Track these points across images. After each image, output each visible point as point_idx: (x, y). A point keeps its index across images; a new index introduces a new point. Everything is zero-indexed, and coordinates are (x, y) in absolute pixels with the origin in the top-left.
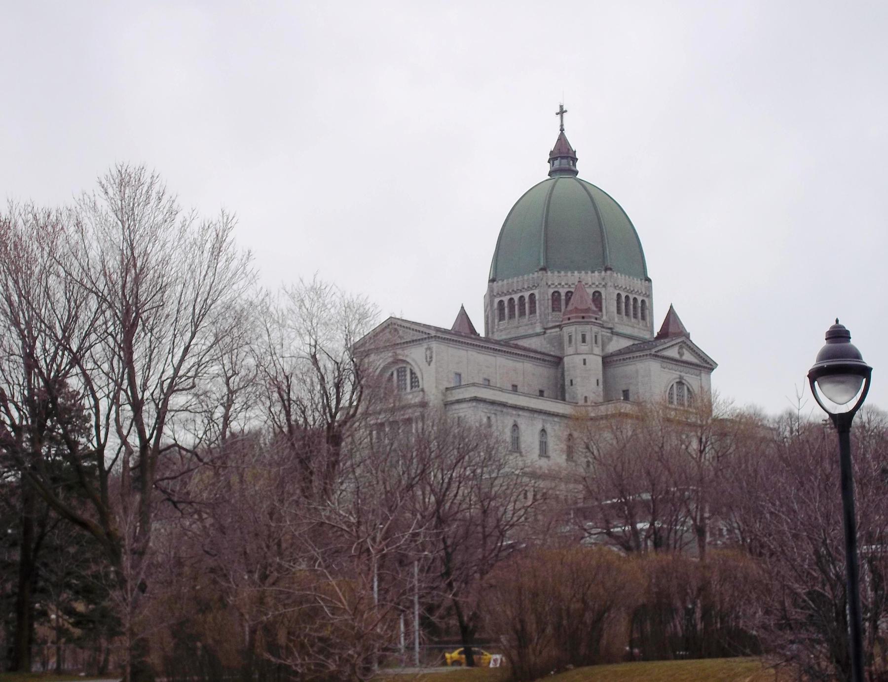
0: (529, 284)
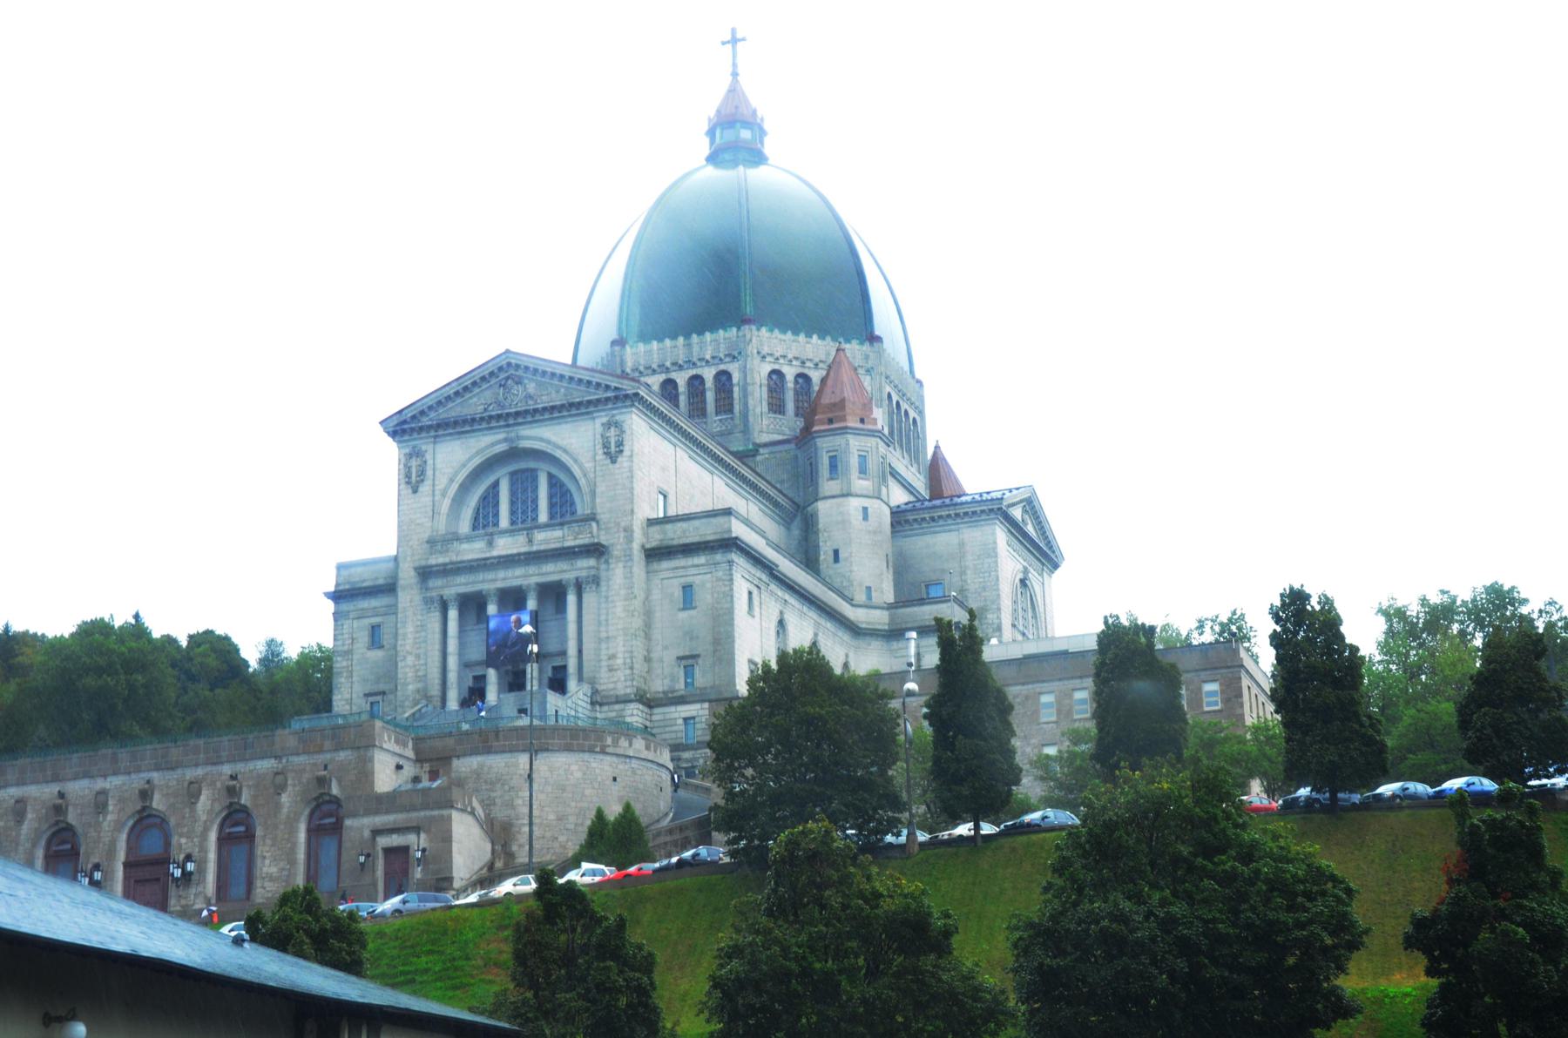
0: (717, 349)
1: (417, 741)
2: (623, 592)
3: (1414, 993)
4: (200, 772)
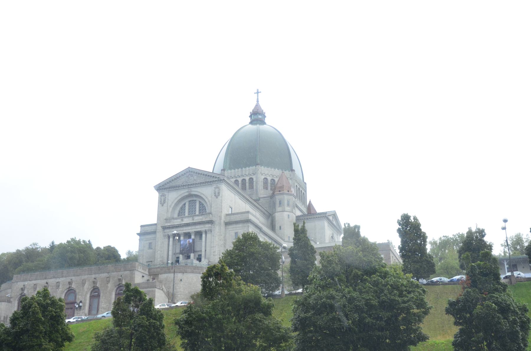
1: (149, 269)
2: (218, 234)
3: (445, 343)
4: (86, 277)
